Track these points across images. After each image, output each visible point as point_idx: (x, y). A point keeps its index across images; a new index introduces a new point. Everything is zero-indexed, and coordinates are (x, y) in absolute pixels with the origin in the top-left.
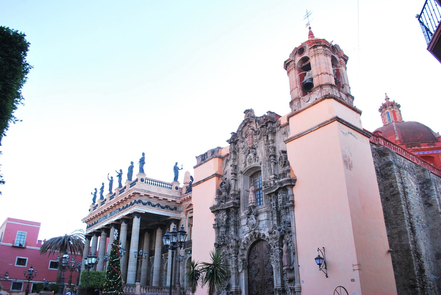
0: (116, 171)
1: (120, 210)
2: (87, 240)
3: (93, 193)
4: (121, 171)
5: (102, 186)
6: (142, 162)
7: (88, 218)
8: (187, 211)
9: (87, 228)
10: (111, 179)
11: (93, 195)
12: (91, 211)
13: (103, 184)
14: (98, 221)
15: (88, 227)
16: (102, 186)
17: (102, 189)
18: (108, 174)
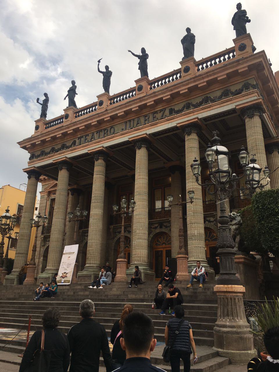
0: (129, 51)
2: (33, 179)
4: (143, 50)
5: (71, 85)
6: (240, 19)
9: (30, 159)
10: (104, 70)
11: (41, 106)
12: (40, 129)
13: (73, 83)
14: (75, 141)
16: (71, 85)
17: (72, 93)
18: (99, 61)
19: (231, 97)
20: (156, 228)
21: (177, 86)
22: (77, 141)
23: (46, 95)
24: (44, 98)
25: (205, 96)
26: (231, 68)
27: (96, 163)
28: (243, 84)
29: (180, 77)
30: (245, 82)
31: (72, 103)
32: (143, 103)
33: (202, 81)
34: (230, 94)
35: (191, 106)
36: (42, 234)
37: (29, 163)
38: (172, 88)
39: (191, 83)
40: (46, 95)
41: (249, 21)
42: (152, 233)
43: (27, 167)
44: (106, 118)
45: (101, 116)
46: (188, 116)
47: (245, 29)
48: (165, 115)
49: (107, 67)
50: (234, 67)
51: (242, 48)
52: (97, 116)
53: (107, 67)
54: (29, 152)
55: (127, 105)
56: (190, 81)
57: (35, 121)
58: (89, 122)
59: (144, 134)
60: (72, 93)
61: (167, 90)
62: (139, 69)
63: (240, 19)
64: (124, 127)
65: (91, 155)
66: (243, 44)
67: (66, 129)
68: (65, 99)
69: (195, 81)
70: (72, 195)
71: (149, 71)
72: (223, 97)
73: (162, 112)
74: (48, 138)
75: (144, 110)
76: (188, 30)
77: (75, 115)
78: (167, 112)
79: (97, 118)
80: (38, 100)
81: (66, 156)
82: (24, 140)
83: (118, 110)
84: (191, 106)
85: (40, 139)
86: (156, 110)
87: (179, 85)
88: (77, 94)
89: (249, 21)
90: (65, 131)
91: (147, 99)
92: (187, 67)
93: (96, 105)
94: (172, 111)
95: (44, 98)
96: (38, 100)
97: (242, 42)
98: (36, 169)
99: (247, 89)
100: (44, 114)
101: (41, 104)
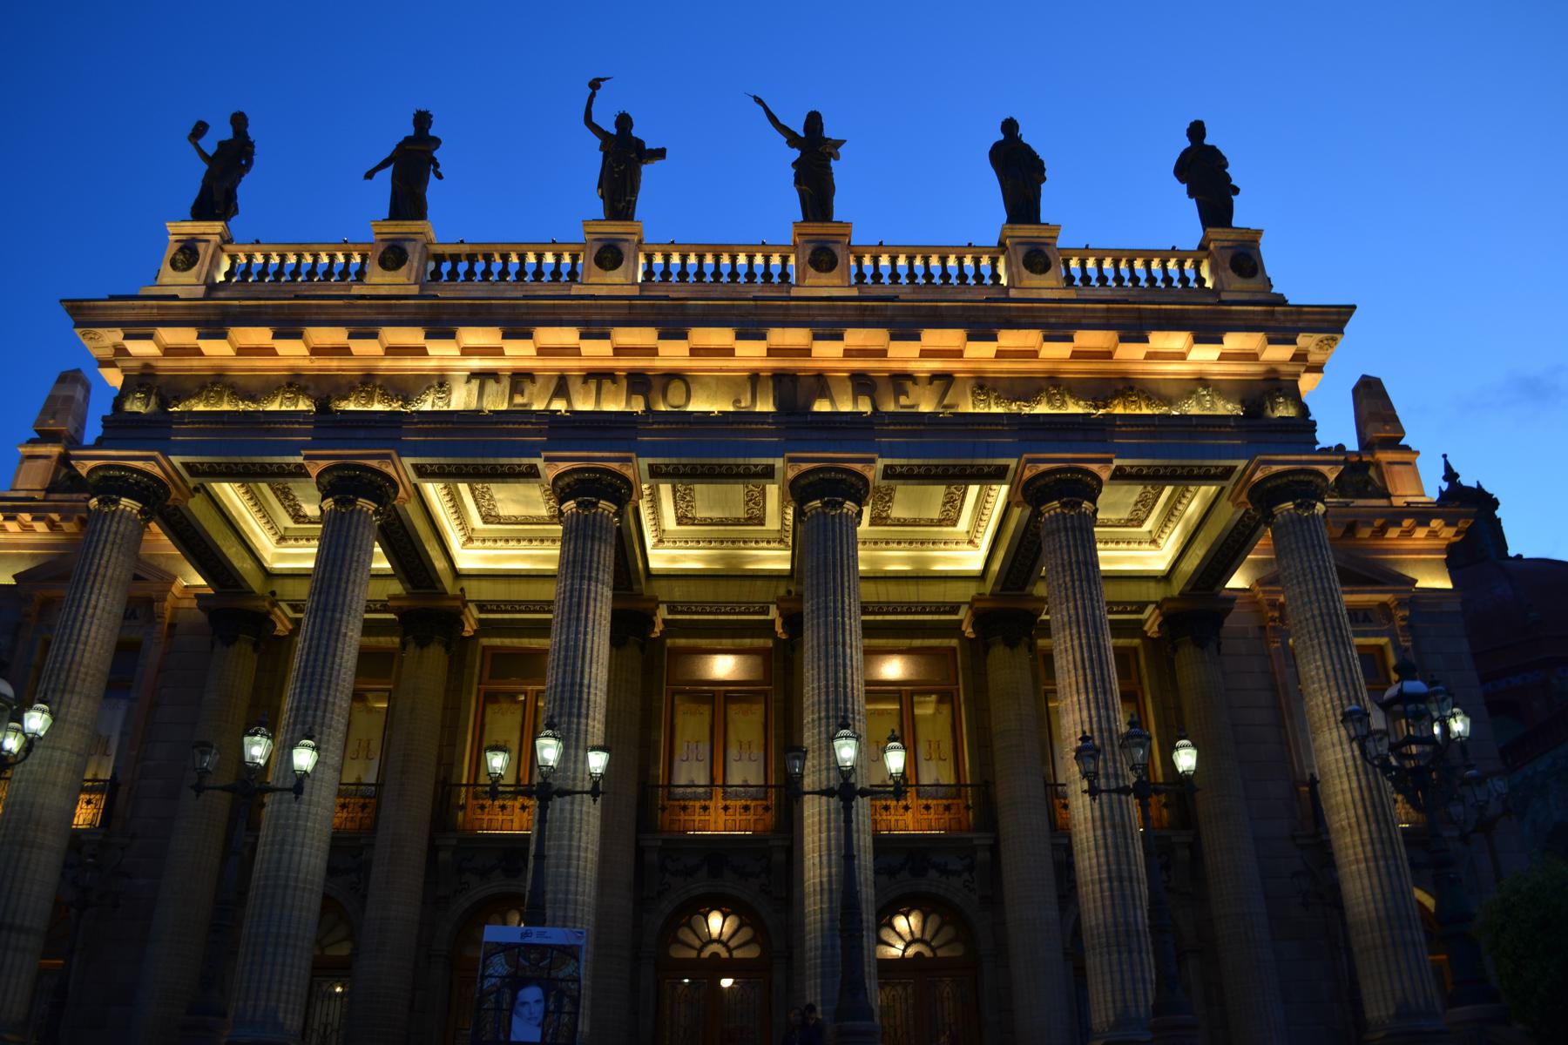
0: (759, 101)
3: (210, 144)
5: (411, 131)
10: (614, 131)
13: (422, 120)
16: (411, 131)
18: (595, 85)
23: (239, 121)
24: (228, 134)
31: (408, 203)
40: (239, 121)
49: (624, 121)
53: (624, 121)
68: (369, 175)
77: (431, 265)
80: (200, 129)
88: (440, 177)
95: (228, 134)
96: (200, 129)
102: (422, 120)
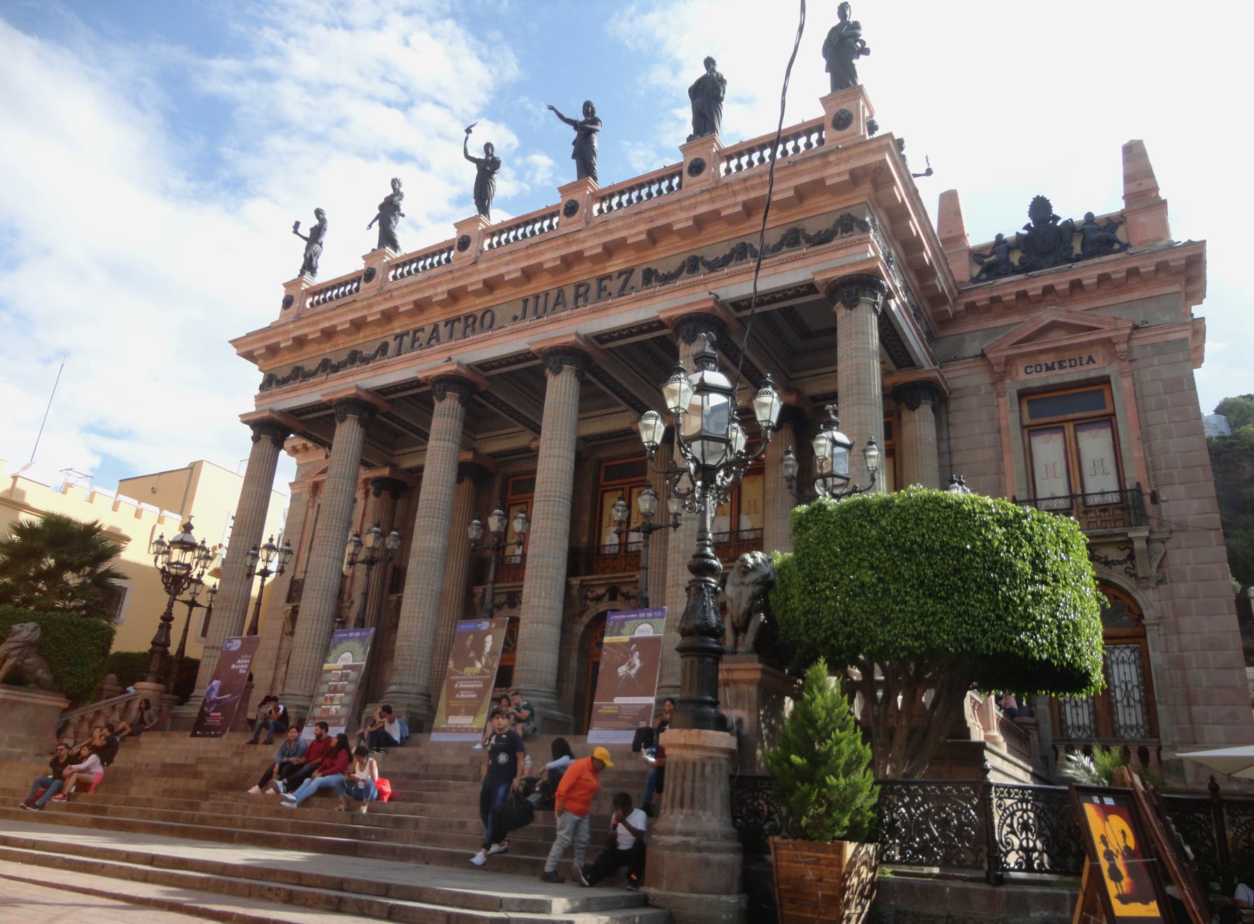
0: (551, 108)
1: (650, 276)
2: (266, 441)
3: (305, 231)
4: (588, 109)
7: (252, 343)
8: (1009, 361)
9: (262, 388)
11: (305, 243)
15: (270, 382)
17: (389, 210)
18: (468, 131)
19: (805, 250)
20: (599, 599)
21: (666, 209)
22: (393, 345)
23: (318, 213)
25: (739, 241)
26: (808, 172)
27: (438, 406)
28: (837, 216)
29: (680, 185)
30: (843, 212)
31: (387, 238)
32: (574, 249)
33: (731, 201)
34: (803, 241)
35: (701, 267)
36: (288, 601)
37: (258, 398)
38: (652, 213)
39: (703, 202)
40: (318, 213)
41: (866, 52)
42: (588, 613)
43: (253, 409)
44: (471, 284)
45: (460, 278)
46: (690, 290)
47: (852, 73)
48: (630, 283)
49: (488, 147)
50: (815, 170)
51: (842, 120)
52: (449, 276)
53: (488, 147)
54: (260, 370)
55: (531, 251)
56: (699, 199)
57: (286, 285)
58: (427, 294)
59: (570, 335)
60: (389, 210)
61: (638, 217)
62: (574, 156)
63: (843, 47)
64: (519, 313)
65: (424, 385)
66: (843, 111)
67: (363, 308)
68: (370, 226)
69: (712, 201)
70: (377, 495)
71: (599, 165)
72: (785, 249)
73: (623, 277)
74: (313, 332)
75: (576, 268)
76: (709, 63)
78: (637, 277)
79: (447, 282)
80: (297, 225)
81: (359, 383)
82: (249, 335)
83: (507, 263)
84: (701, 267)
85: (292, 335)
86: (608, 271)
87: (670, 208)
89: (866, 52)
90: (359, 314)
91: (585, 241)
92: (696, 160)
93: (450, 249)
94: (650, 276)
96: (297, 225)
97: (844, 107)
98: (276, 417)
99: (847, 232)
100: (309, 266)
101: (305, 238)
102: (395, 182)
